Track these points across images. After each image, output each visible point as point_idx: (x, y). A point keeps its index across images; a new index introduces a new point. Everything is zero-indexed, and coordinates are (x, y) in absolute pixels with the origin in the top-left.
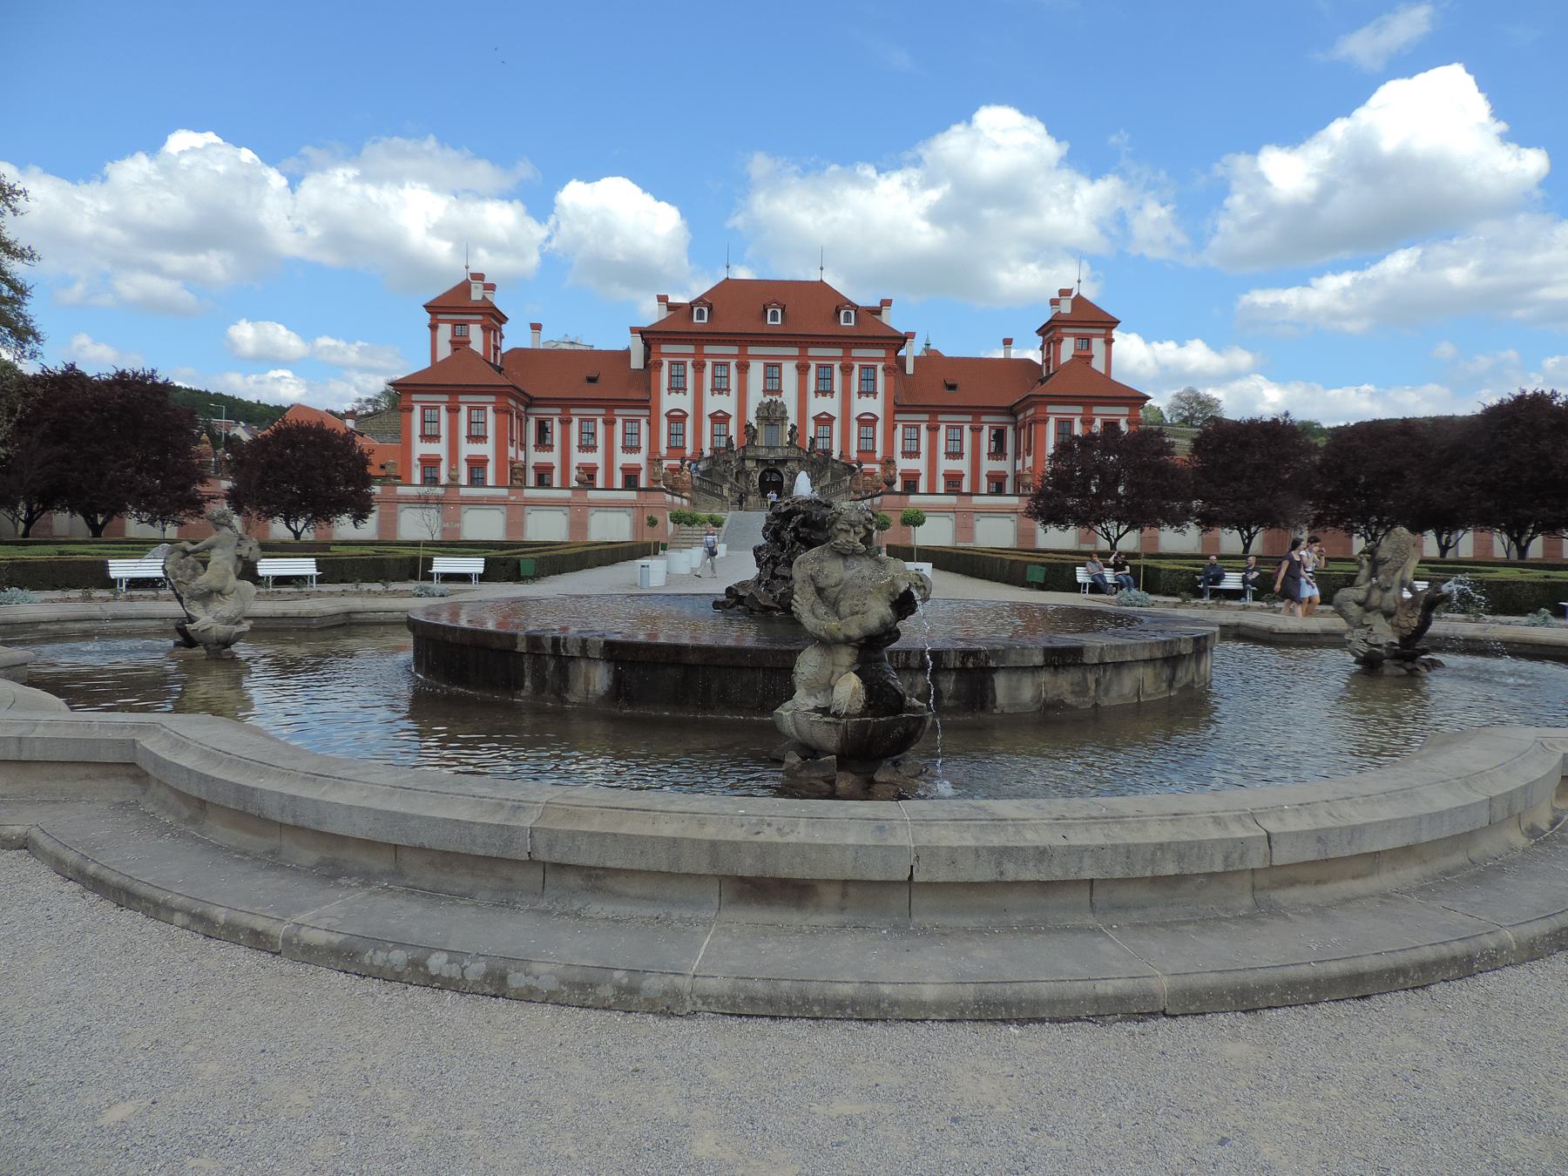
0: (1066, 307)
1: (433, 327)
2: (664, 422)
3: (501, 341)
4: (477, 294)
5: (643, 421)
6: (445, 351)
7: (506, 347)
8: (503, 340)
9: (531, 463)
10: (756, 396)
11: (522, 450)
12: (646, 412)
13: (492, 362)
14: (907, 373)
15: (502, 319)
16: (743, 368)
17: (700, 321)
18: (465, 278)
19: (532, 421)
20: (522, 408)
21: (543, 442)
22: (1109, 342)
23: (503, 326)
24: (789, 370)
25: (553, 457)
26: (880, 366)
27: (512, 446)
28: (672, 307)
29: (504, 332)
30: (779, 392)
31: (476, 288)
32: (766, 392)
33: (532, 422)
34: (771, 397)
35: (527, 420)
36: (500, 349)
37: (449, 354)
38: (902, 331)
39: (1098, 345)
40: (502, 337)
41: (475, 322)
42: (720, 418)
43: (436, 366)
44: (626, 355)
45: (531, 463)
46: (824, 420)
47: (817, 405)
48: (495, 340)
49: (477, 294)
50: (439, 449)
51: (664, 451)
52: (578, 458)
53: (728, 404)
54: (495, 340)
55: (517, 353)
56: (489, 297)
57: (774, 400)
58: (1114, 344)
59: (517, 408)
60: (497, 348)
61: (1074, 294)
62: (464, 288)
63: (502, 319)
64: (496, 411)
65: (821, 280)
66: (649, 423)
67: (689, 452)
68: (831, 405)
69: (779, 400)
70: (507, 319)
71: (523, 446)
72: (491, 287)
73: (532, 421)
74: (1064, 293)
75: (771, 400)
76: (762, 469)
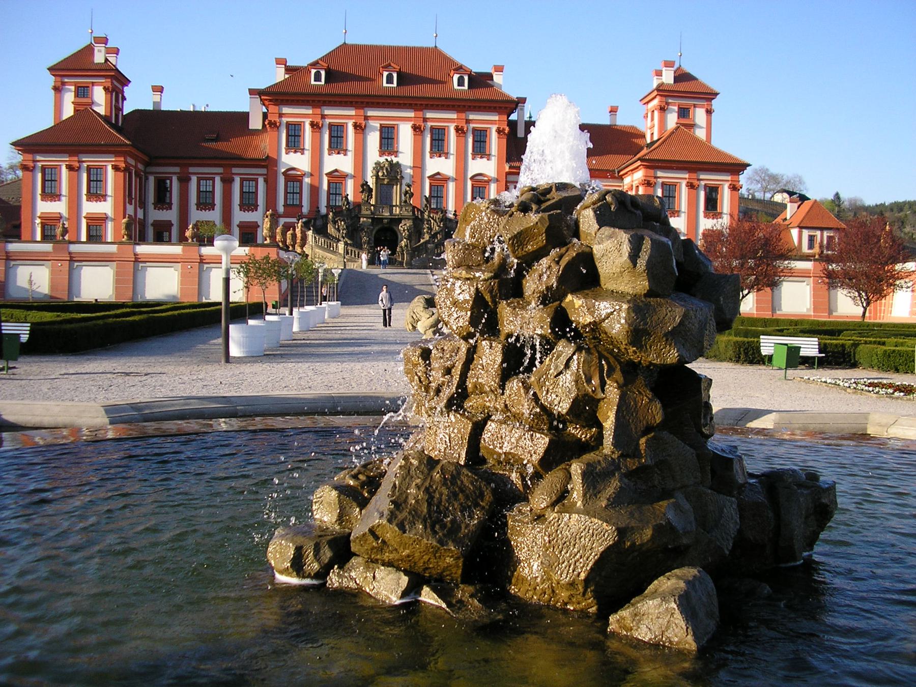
0: (668, 77)
1: (58, 89)
2: (281, 180)
3: (123, 103)
4: (99, 57)
5: (261, 181)
6: (68, 111)
7: (128, 108)
8: (125, 102)
9: (150, 220)
10: (373, 155)
11: (141, 208)
12: (264, 171)
13: (113, 122)
14: (519, 136)
15: (125, 82)
16: (360, 129)
17: (316, 82)
18: (89, 43)
19: (152, 179)
20: (140, 166)
21: (162, 201)
22: (709, 112)
23: (126, 88)
24: (405, 134)
25: (171, 215)
26: (494, 128)
27: (131, 204)
28: (289, 70)
29: (126, 94)
30: (396, 153)
31: (100, 51)
32: (382, 153)
33: (151, 181)
34: (386, 157)
35: (147, 179)
36: (122, 110)
37: (72, 114)
38: (514, 95)
39: (700, 115)
40: (124, 99)
41: (99, 84)
42: (337, 178)
43: (60, 126)
44: (244, 117)
45: (150, 220)
46: (439, 181)
47: (435, 165)
48: (117, 100)
49: (99, 57)
50: (60, 207)
51: (281, 209)
52: (196, 215)
53: (343, 163)
54: (117, 100)
55: (139, 114)
56: (112, 59)
57: (389, 160)
58: (713, 114)
59: (136, 167)
60: (119, 109)
61: (676, 66)
62: (88, 51)
63: (125, 82)
64: (116, 168)
65: (436, 47)
66: (266, 181)
67: (305, 210)
68: (444, 166)
69: (395, 160)
70: (130, 81)
71: (143, 204)
72: (116, 51)
73: (152, 179)
74: (669, 64)
75: (387, 160)
76: (377, 228)
